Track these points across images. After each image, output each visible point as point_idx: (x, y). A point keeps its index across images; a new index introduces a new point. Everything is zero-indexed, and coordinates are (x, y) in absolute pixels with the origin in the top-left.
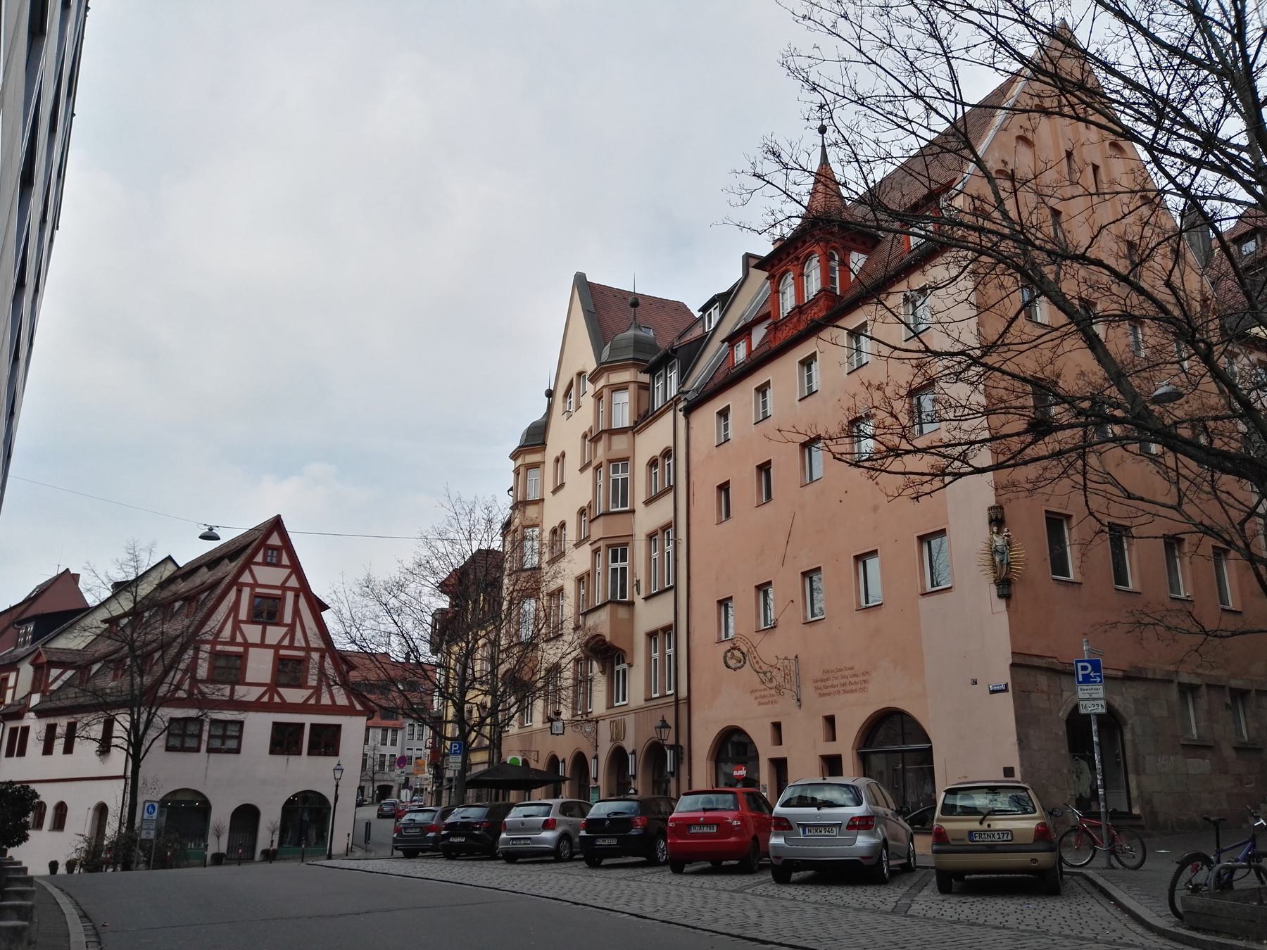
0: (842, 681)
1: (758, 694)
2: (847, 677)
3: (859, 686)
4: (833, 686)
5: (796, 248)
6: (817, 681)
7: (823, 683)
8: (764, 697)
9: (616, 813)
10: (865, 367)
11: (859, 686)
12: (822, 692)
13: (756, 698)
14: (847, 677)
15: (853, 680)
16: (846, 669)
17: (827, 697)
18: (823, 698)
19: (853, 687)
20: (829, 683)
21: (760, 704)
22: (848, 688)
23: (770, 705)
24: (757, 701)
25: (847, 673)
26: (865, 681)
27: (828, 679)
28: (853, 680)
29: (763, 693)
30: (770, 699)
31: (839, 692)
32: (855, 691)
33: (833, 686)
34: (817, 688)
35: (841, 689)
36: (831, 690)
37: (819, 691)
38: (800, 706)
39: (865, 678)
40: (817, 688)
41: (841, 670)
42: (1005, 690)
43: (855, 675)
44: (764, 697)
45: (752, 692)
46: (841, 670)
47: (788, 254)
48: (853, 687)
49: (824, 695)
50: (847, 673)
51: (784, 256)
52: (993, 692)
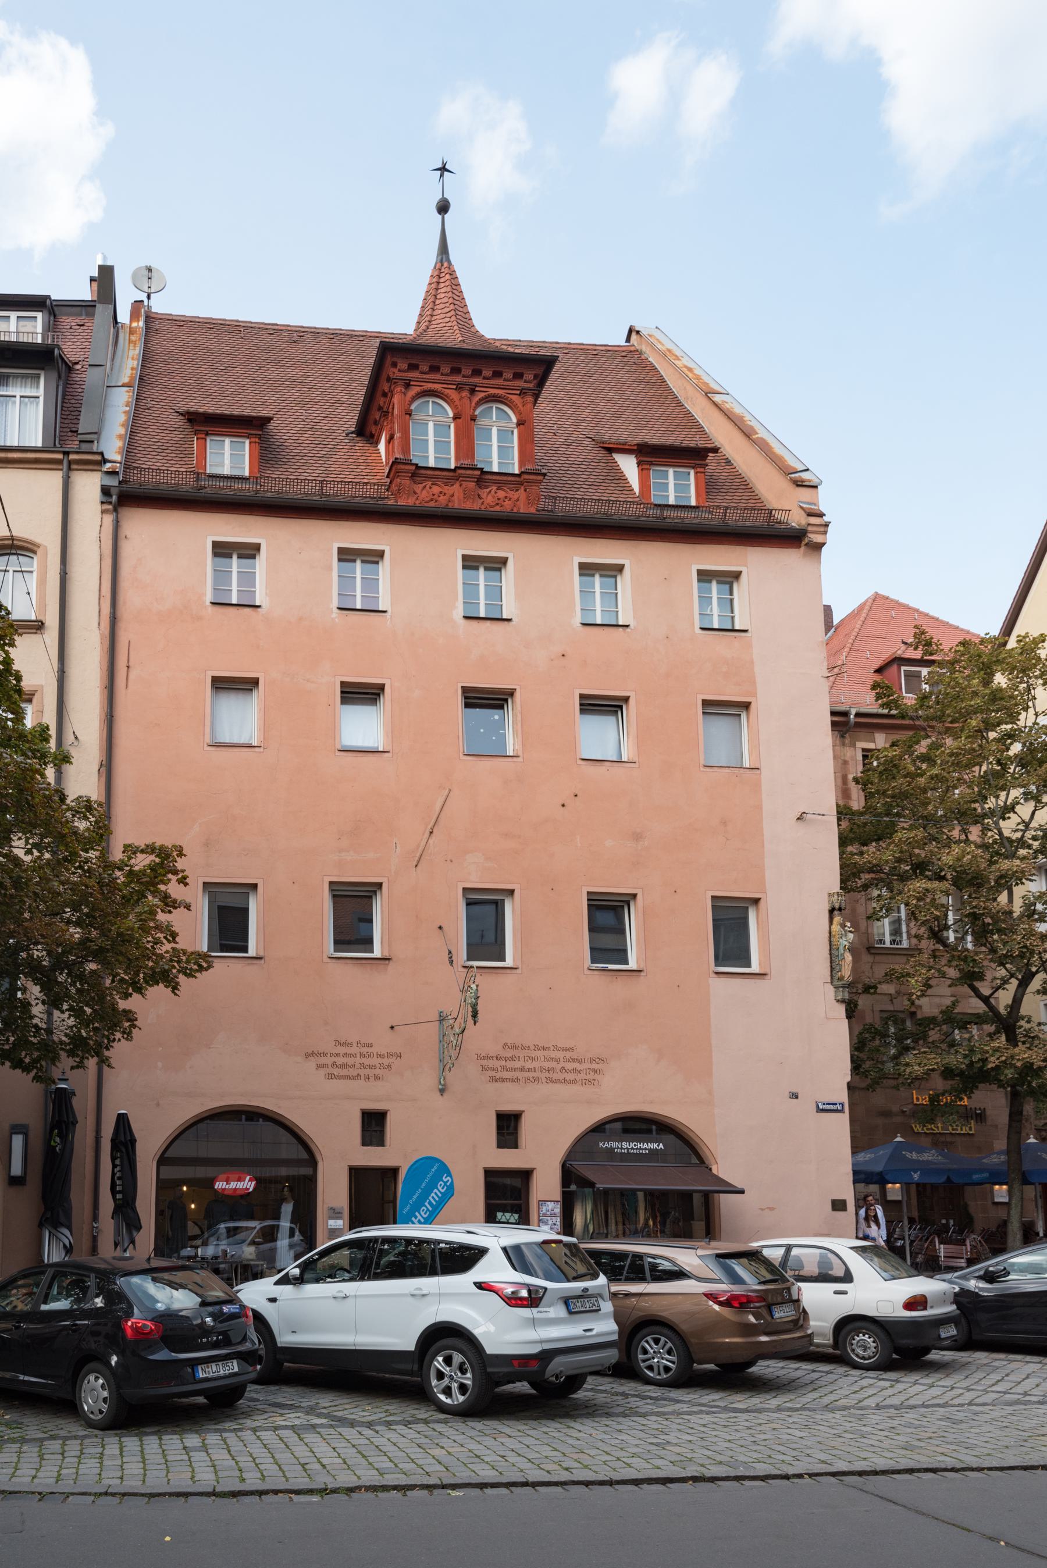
0: (547, 1065)
1: (329, 1060)
2: (558, 1061)
3: (582, 1076)
4: (523, 1069)
5: (477, 372)
6: (487, 1058)
7: (503, 1063)
8: (344, 1066)
9: (23, 1271)
10: (621, 629)
11: (582, 1076)
12: (498, 1075)
13: (320, 1066)
14: (558, 1061)
15: (570, 1066)
16: (556, 1048)
17: (509, 1084)
18: (498, 1085)
19: (570, 1077)
20: (518, 1064)
21: (331, 1076)
22: (555, 1076)
23: (361, 1082)
24: (322, 1072)
25: (560, 1055)
26: (595, 1071)
27: (512, 1058)
28: (570, 1066)
29: (340, 1061)
30: (362, 1072)
31: (537, 1080)
32: (574, 1082)
33: (523, 1069)
34: (484, 1068)
35: (543, 1076)
36: (521, 1075)
37: (493, 1073)
38: (442, 1091)
39: (595, 1066)
40: (484, 1068)
41: (544, 1049)
42: (842, 1111)
43: (574, 1060)
44: (344, 1066)
45: (307, 1055)
46: (544, 1049)
47: (456, 371)
48: (570, 1077)
49: (502, 1080)
50: (560, 1055)
51: (446, 369)
52: (820, 1110)
